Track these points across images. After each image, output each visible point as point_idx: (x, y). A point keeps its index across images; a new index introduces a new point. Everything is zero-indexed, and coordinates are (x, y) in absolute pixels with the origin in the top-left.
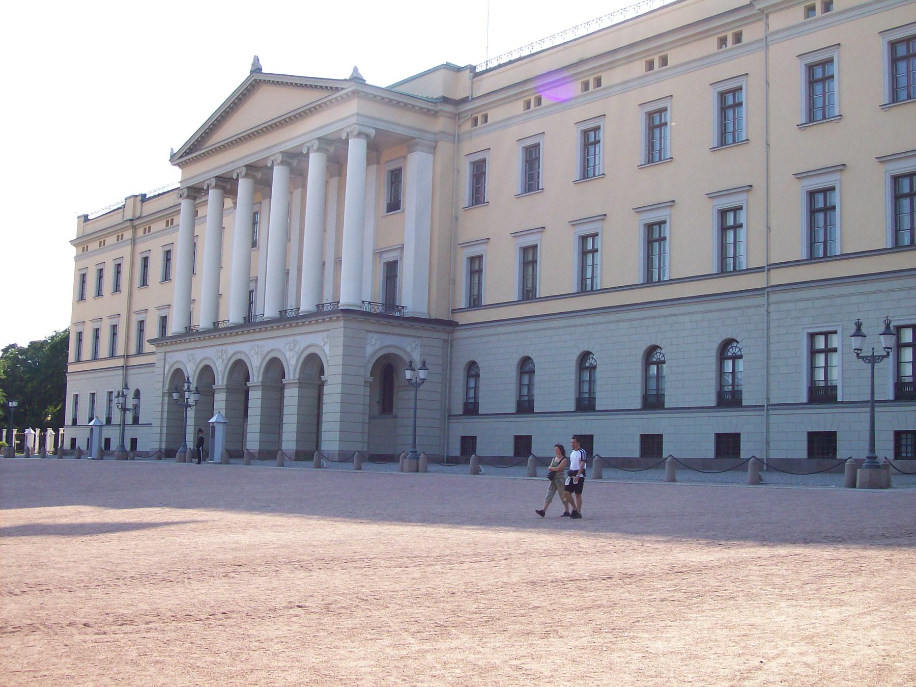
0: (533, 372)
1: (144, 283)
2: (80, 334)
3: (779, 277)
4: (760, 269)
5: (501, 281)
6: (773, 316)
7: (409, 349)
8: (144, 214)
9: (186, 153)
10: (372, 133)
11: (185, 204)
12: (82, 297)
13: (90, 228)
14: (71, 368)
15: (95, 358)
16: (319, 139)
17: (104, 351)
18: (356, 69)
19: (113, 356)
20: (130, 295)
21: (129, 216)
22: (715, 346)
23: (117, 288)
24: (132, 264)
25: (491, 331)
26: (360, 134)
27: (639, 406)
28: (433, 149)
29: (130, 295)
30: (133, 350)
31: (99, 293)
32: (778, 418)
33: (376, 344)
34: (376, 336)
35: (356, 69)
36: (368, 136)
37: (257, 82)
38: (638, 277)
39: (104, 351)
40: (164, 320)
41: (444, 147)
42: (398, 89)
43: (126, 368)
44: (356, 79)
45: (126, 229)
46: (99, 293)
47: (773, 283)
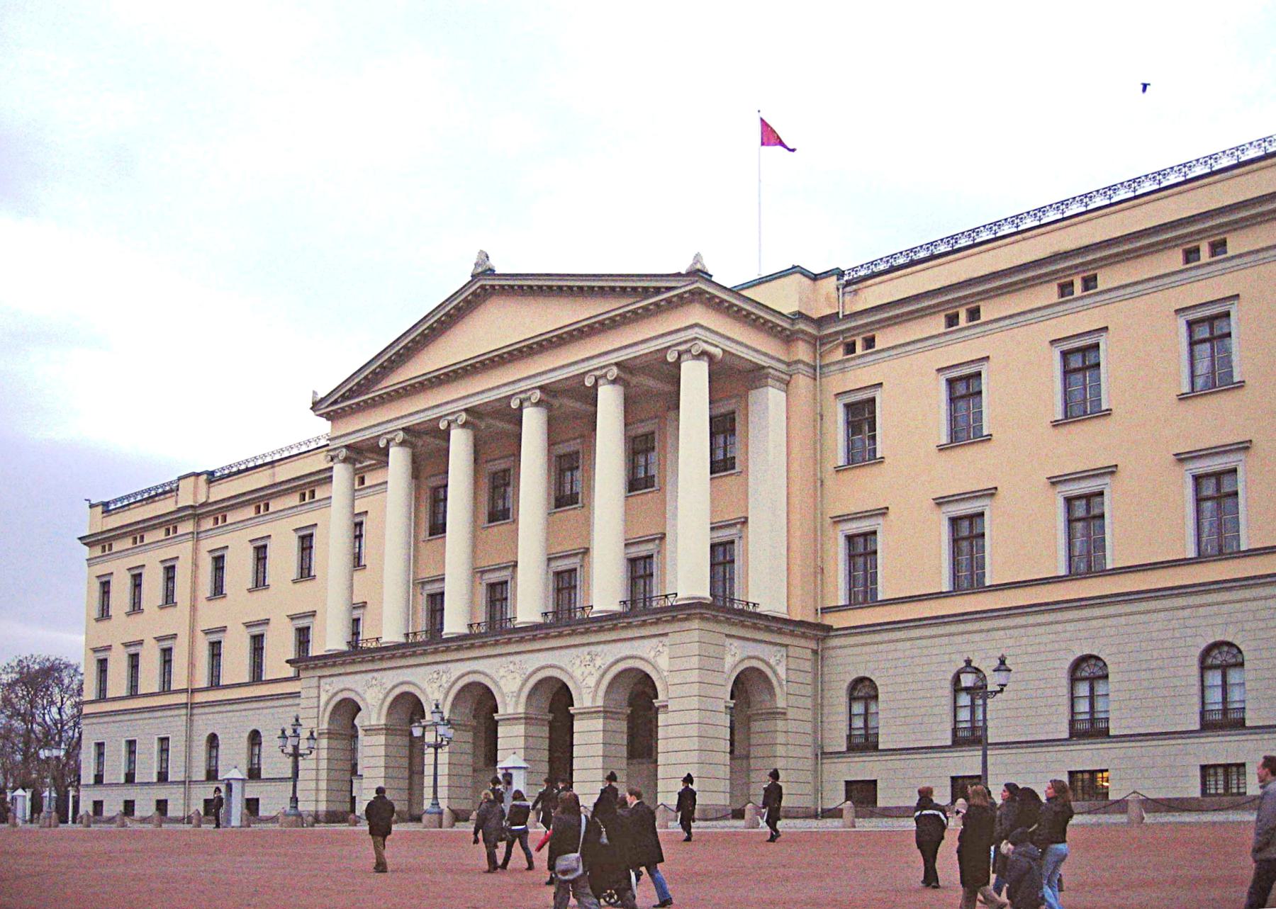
1: (218, 590)
7: (772, 661)
10: (717, 352)
11: (341, 473)
12: (104, 614)
13: (115, 521)
15: (133, 693)
17: (149, 680)
18: (697, 258)
19: (166, 689)
20: (194, 608)
23: (169, 599)
24: (195, 565)
28: (786, 385)
29: (194, 608)
30: (202, 681)
31: (136, 607)
33: (736, 654)
34: (736, 643)
35: (697, 258)
36: (711, 357)
39: (149, 680)
41: (802, 382)
44: (698, 273)
46: (136, 607)
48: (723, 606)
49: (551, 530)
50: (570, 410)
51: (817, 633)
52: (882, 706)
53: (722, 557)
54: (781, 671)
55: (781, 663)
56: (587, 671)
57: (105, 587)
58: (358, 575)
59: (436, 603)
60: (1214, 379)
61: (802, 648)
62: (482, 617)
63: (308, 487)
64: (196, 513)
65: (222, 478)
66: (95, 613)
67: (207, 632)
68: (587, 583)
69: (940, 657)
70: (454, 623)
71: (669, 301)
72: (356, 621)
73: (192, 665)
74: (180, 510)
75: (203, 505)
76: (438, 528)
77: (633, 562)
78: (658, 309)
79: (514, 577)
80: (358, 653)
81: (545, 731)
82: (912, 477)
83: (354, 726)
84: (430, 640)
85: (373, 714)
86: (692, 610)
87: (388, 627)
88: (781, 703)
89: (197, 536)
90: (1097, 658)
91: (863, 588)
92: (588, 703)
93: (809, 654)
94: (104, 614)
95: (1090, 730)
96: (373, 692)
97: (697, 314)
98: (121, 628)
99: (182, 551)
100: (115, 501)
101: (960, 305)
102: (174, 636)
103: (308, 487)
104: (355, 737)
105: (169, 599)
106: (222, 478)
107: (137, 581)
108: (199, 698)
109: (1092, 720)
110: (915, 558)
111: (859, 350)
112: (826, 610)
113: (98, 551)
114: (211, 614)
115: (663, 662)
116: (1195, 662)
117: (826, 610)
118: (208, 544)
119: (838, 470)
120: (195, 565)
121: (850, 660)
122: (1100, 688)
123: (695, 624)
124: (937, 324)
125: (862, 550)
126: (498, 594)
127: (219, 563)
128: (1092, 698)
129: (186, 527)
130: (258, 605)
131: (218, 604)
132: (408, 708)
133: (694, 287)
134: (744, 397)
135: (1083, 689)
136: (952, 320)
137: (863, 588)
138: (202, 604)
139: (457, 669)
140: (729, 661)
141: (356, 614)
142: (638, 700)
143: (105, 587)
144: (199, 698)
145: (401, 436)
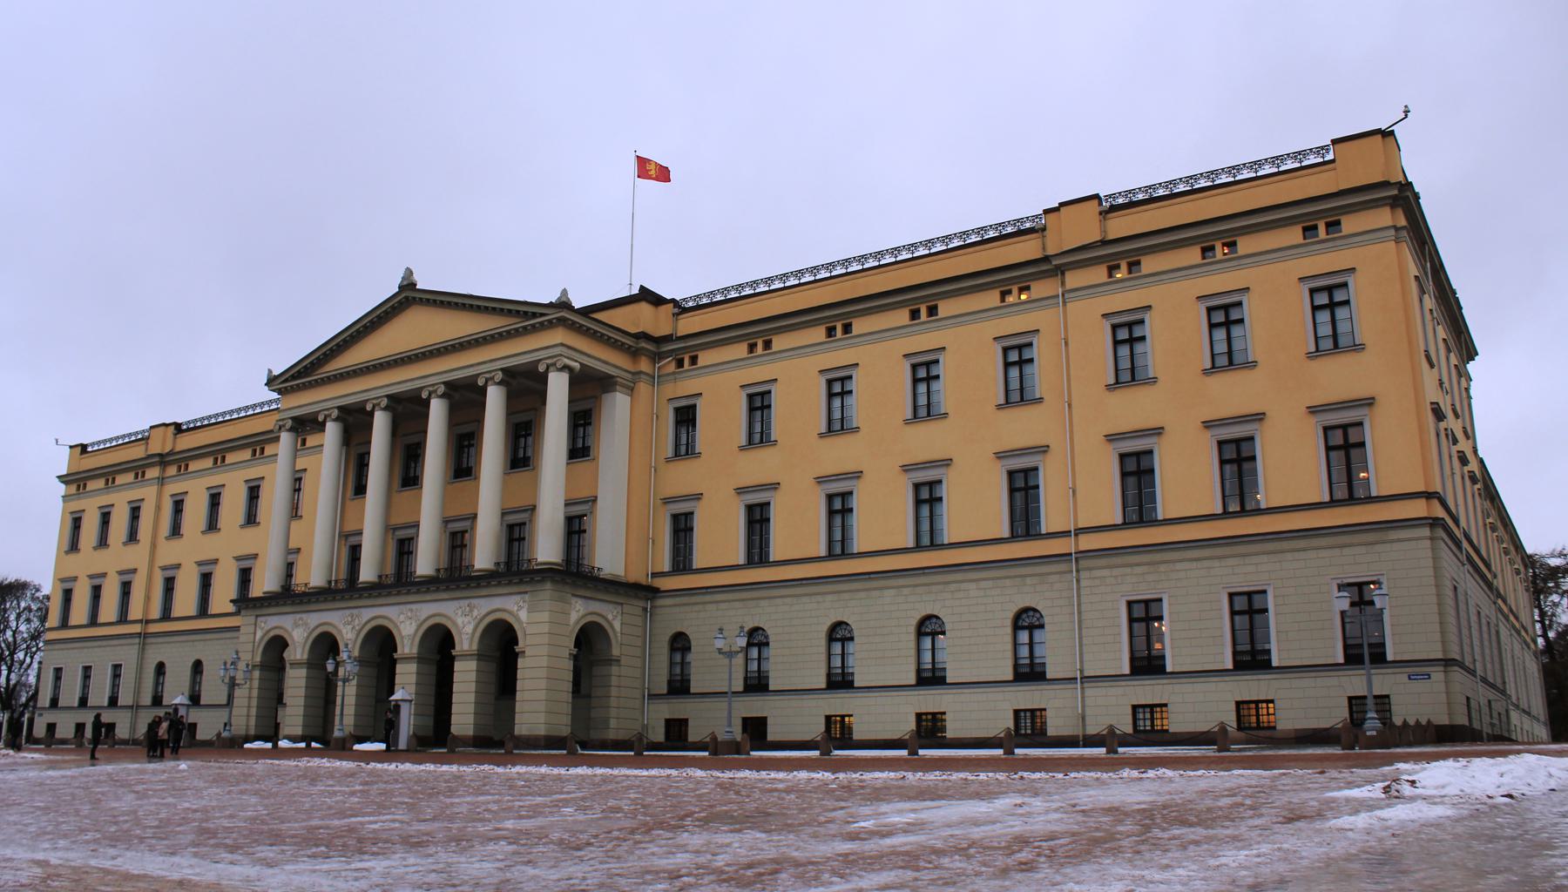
0: (767, 644)
1: (176, 531)
2: (68, 595)
3: (1087, 542)
4: (1066, 534)
5: (720, 538)
6: (1083, 583)
7: (610, 617)
8: (178, 449)
10: (576, 365)
12: (74, 547)
15: (93, 621)
16: (502, 370)
17: (109, 610)
19: (123, 619)
20: (154, 546)
23: (133, 537)
24: (158, 508)
25: (708, 598)
26: (565, 368)
27: (913, 682)
29: (154, 546)
30: (156, 613)
32: (1094, 693)
37: (409, 297)
39: (109, 610)
42: (614, 317)
43: (144, 636)
46: (103, 542)
47: (1082, 548)
48: (574, 572)
49: (446, 498)
50: (465, 399)
52: (772, 652)
53: (575, 529)
54: (617, 625)
55: (615, 617)
56: (466, 619)
57: (77, 523)
58: (294, 524)
59: (355, 552)
60: (1018, 396)
61: (635, 606)
62: (390, 569)
63: (258, 444)
64: (163, 460)
65: (189, 429)
66: (66, 547)
67: (164, 568)
68: (532, 534)
69: (825, 610)
70: (367, 573)
71: (541, 323)
72: (290, 565)
73: (148, 599)
74: (149, 456)
75: (168, 454)
76: (360, 489)
77: (511, 527)
78: (534, 329)
79: (473, 528)
80: (288, 596)
81: (433, 669)
82: (719, 476)
83: (282, 659)
84: (346, 589)
85: (298, 651)
86: (548, 573)
87: (313, 574)
88: (616, 652)
89: (162, 481)
90: (1035, 610)
91: (682, 561)
92: (466, 647)
93: (639, 611)
94: (74, 547)
95: (931, 678)
96: (299, 630)
97: (558, 336)
98: (89, 560)
99: (148, 493)
100: (93, 444)
102: (134, 571)
103: (258, 444)
104: (283, 669)
105: (133, 537)
106: (189, 429)
107: (105, 518)
108: (153, 628)
109: (1032, 664)
110: (720, 538)
113: (73, 489)
114: (170, 552)
115: (523, 615)
116: (912, 629)
117: (654, 575)
118: (174, 488)
120: (158, 508)
121: (674, 617)
122: (1038, 635)
123: (548, 586)
125: (682, 527)
126: (405, 549)
127: (178, 506)
128: (1031, 644)
129: (153, 473)
130: (212, 546)
131: (176, 544)
132: (326, 645)
133: (561, 313)
135: (837, 648)
137: (682, 561)
139: (367, 614)
140: (574, 617)
141: (291, 558)
142: (502, 644)
143: (77, 523)
144: (153, 628)
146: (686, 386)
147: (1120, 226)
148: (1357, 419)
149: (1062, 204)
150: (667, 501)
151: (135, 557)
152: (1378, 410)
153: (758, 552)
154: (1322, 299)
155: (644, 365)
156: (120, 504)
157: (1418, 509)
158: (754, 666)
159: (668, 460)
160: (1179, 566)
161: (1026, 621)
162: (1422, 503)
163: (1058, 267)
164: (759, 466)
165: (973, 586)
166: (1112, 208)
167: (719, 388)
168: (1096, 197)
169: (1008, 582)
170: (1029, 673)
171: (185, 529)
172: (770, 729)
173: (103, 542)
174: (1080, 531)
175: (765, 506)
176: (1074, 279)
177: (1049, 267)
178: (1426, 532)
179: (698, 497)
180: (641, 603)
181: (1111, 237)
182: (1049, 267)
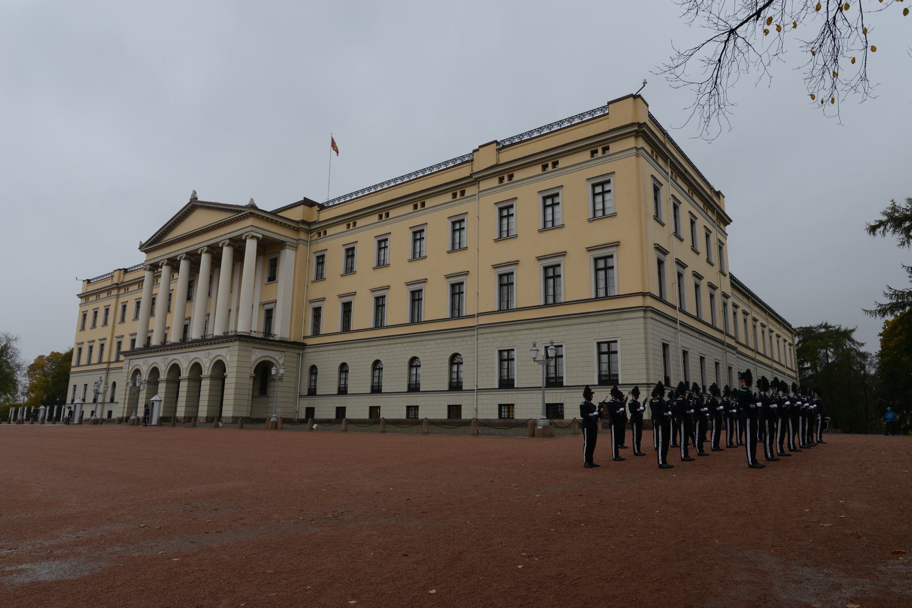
1: (123, 320)
2: (80, 349)
3: (483, 320)
5: (331, 320)
6: (480, 341)
9: (150, 245)
10: (260, 236)
11: (147, 275)
14: (72, 370)
15: (89, 364)
17: (95, 359)
18: (252, 200)
19: (100, 362)
20: (114, 327)
21: (115, 281)
22: (448, 357)
23: (106, 323)
24: (116, 309)
26: (253, 237)
29: (114, 327)
30: (113, 359)
31: (94, 326)
35: (252, 200)
36: (257, 238)
37: (195, 205)
38: (371, 325)
39: (95, 359)
40: (134, 341)
41: (301, 247)
44: (253, 206)
45: (113, 289)
46: (94, 326)
51: (300, 346)
57: (85, 315)
61: (293, 353)
73: (110, 351)
93: (296, 355)
97: (250, 222)
99: (112, 302)
101: (548, 160)
102: (105, 339)
108: (112, 366)
110: (331, 320)
111: (458, 196)
112: (304, 337)
114: (121, 330)
119: (313, 282)
120: (116, 309)
124: (538, 169)
127: (124, 307)
129: (114, 292)
131: (123, 325)
133: (252, 211)
134: (279, 252)
136: (455, 195)
138: (117, 325)
143: (85, 315)
144: (112, 366)
145: (184, 255)
146: (321, 245)
147: (507, 156)
148: (610, 254)
149: (480, 147)
150: (311, 302)
151: (105, 332)
152: (621, 249)
153: (346, 326)
154: (599, 190)
155: (302, 236)
156: (101, 306)
157: (638, 302)
158: (343, 382)
159: (313, 282)
160: (522, 332)
161: (455, 360)
162: (640, 298)
163: (476, 179)
164: (348, 284)
165: (433, 342)
166: (501, 146)
167: (334, 245)
168: (496, 142)
169: (448, 340)
170: (455, 386)
171: (126, 320)
172: (347, 413)
173: (94, 326)
174: (480, 314)
175: (350, 303)
176: (484, 185)
177: (474, 180)
178: (641, 314)
179: (323, 299)
180: (298, 351)
181: (501, 162)
182: (474, 180)
